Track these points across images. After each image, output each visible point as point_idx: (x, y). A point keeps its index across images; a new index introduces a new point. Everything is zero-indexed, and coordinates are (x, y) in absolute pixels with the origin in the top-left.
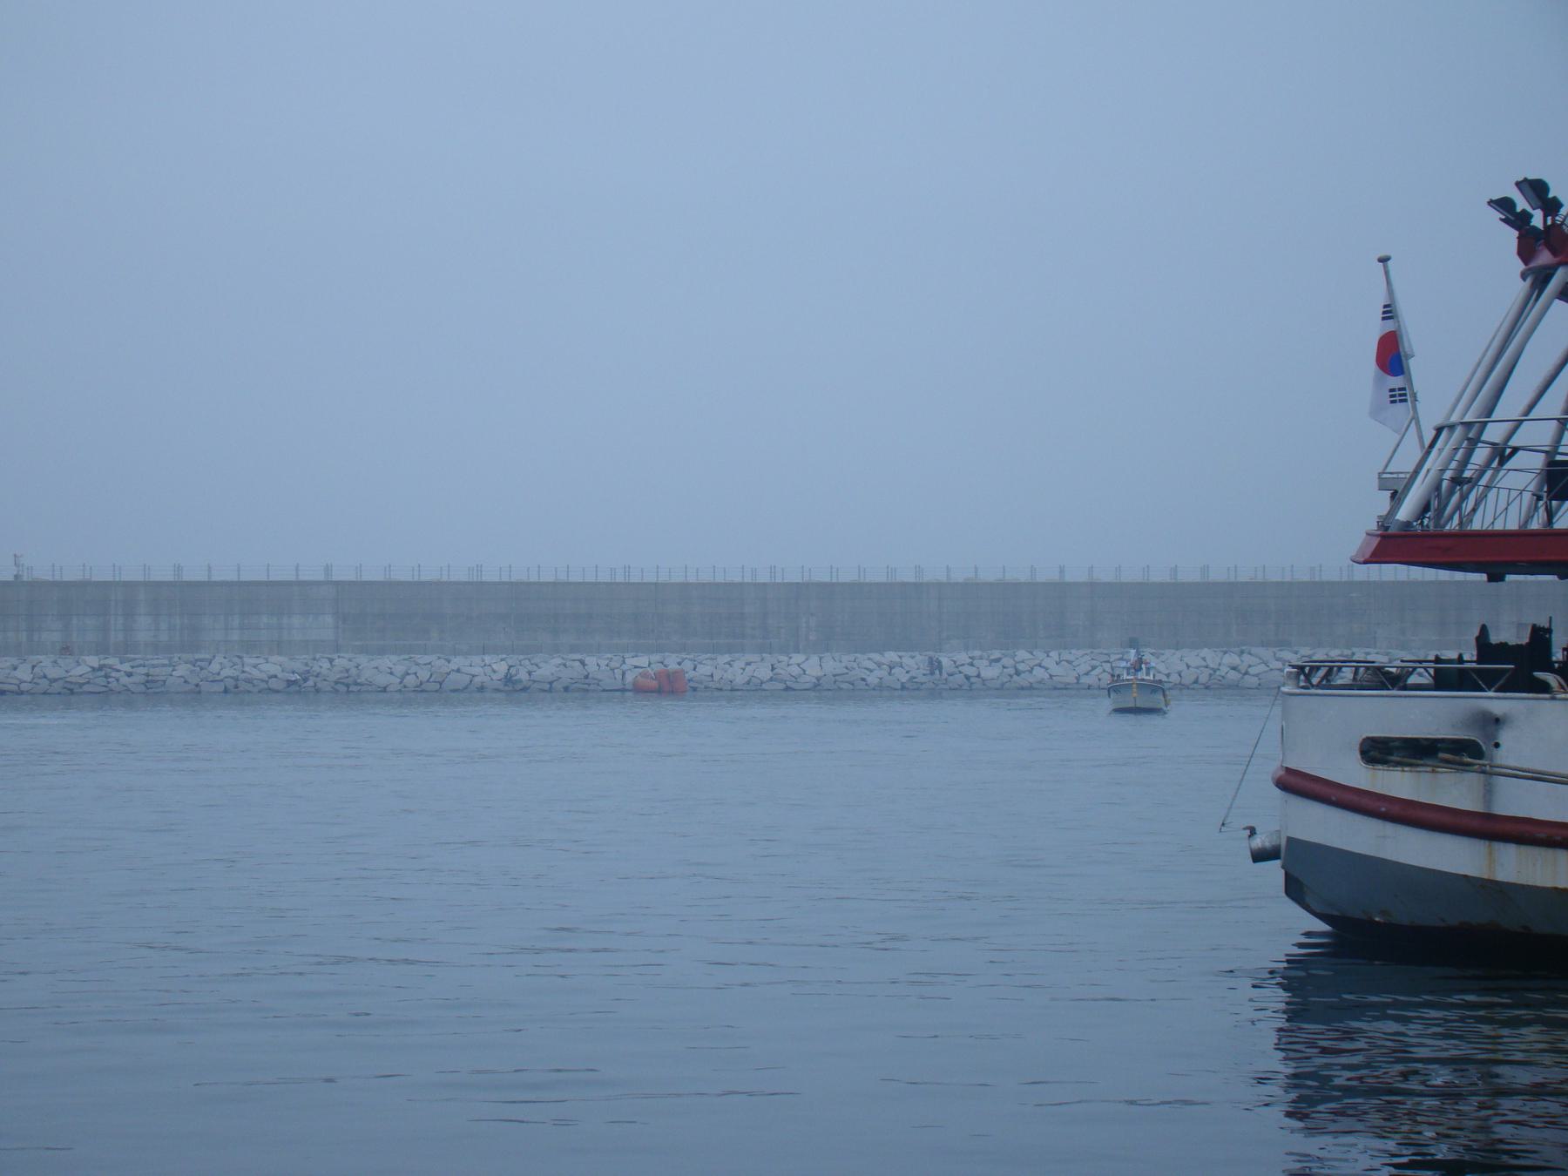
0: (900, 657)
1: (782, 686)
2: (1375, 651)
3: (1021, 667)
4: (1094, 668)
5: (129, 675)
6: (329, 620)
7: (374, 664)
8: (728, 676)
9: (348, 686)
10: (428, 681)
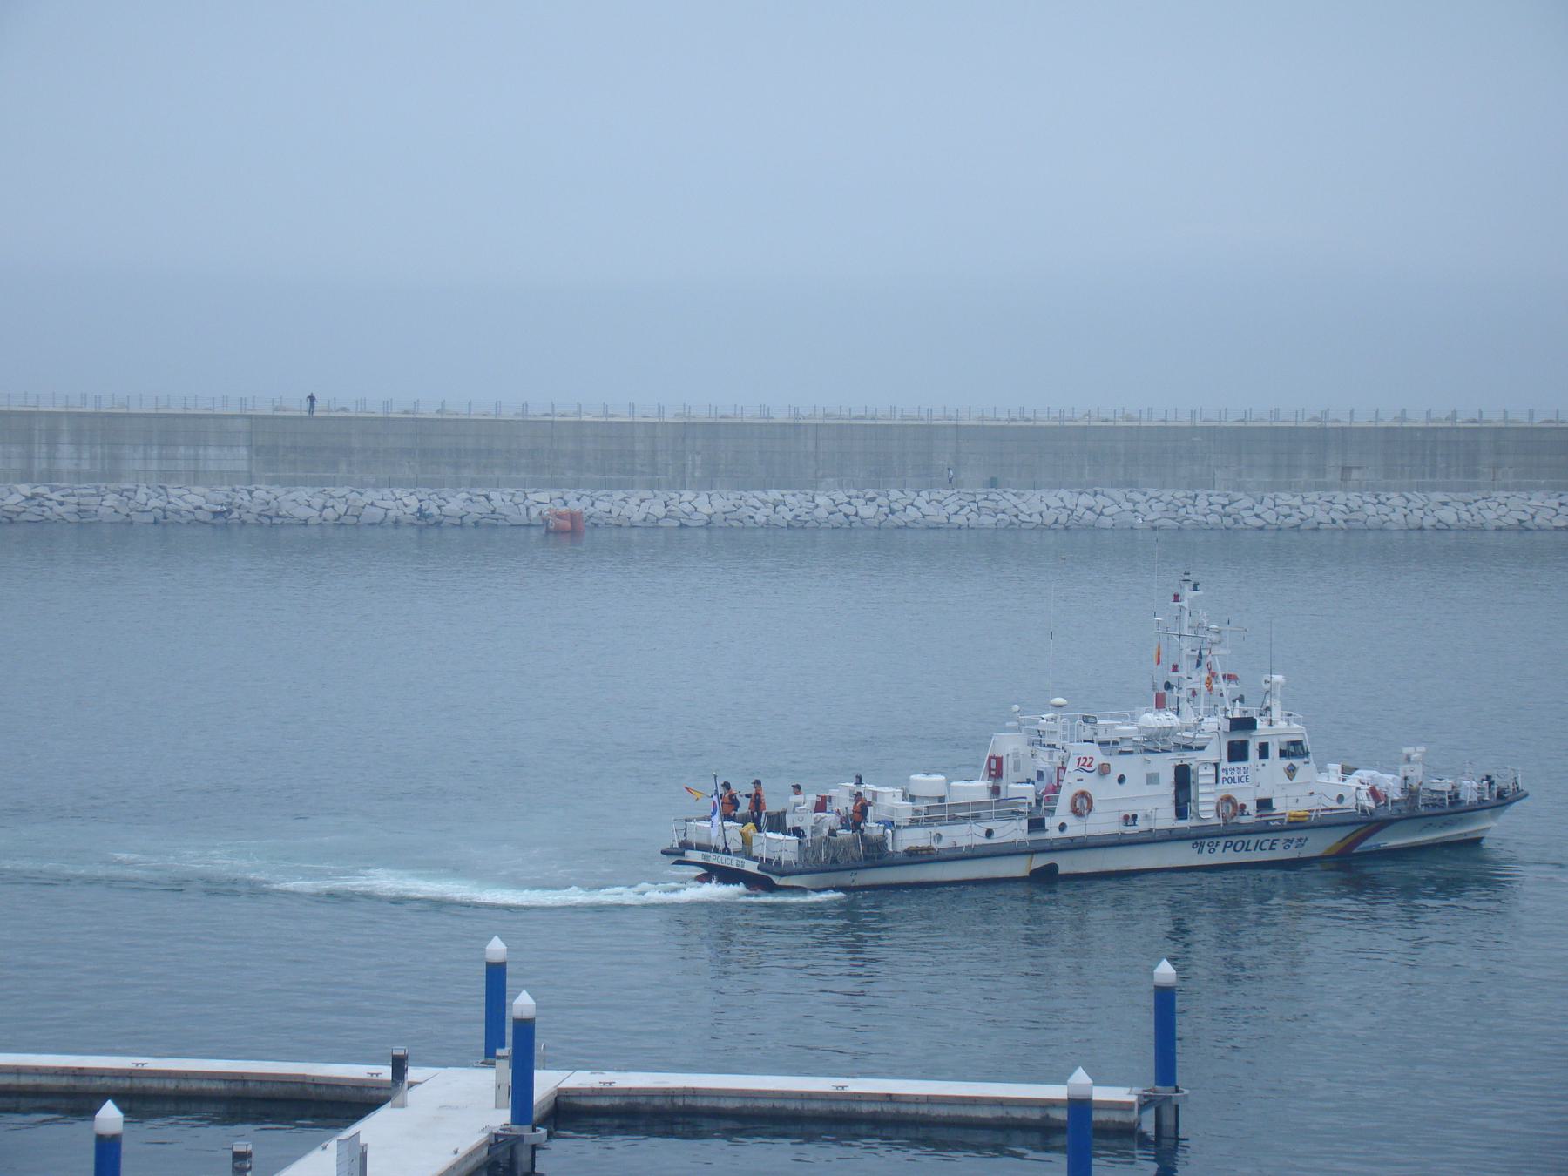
0: (783, 495)
1: (677, 523)
2: (1216, 492)
3: (896, 506)
4: (962, 507)
5: (61, 504)
6: (243, 452)
7: (292, 496)
8: (626, 512)
9: (270, 518)
10: (345, 514)
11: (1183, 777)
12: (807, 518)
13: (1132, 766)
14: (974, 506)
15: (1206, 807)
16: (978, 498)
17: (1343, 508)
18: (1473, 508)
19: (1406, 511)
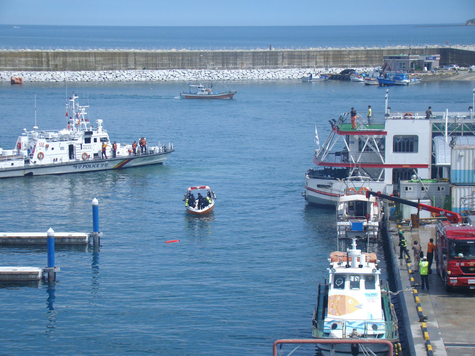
1: (55, 81)
3: (118, 75)
4: (136, 75)
8: (40, 78)
11: (71, 148)
12: (92, 79)
13: (56, 145)
14: (140, 75)
15: (79, 155)
16: (141, 72)
17: (242, 74)
18: (276, 74)
19: (258, 75)
